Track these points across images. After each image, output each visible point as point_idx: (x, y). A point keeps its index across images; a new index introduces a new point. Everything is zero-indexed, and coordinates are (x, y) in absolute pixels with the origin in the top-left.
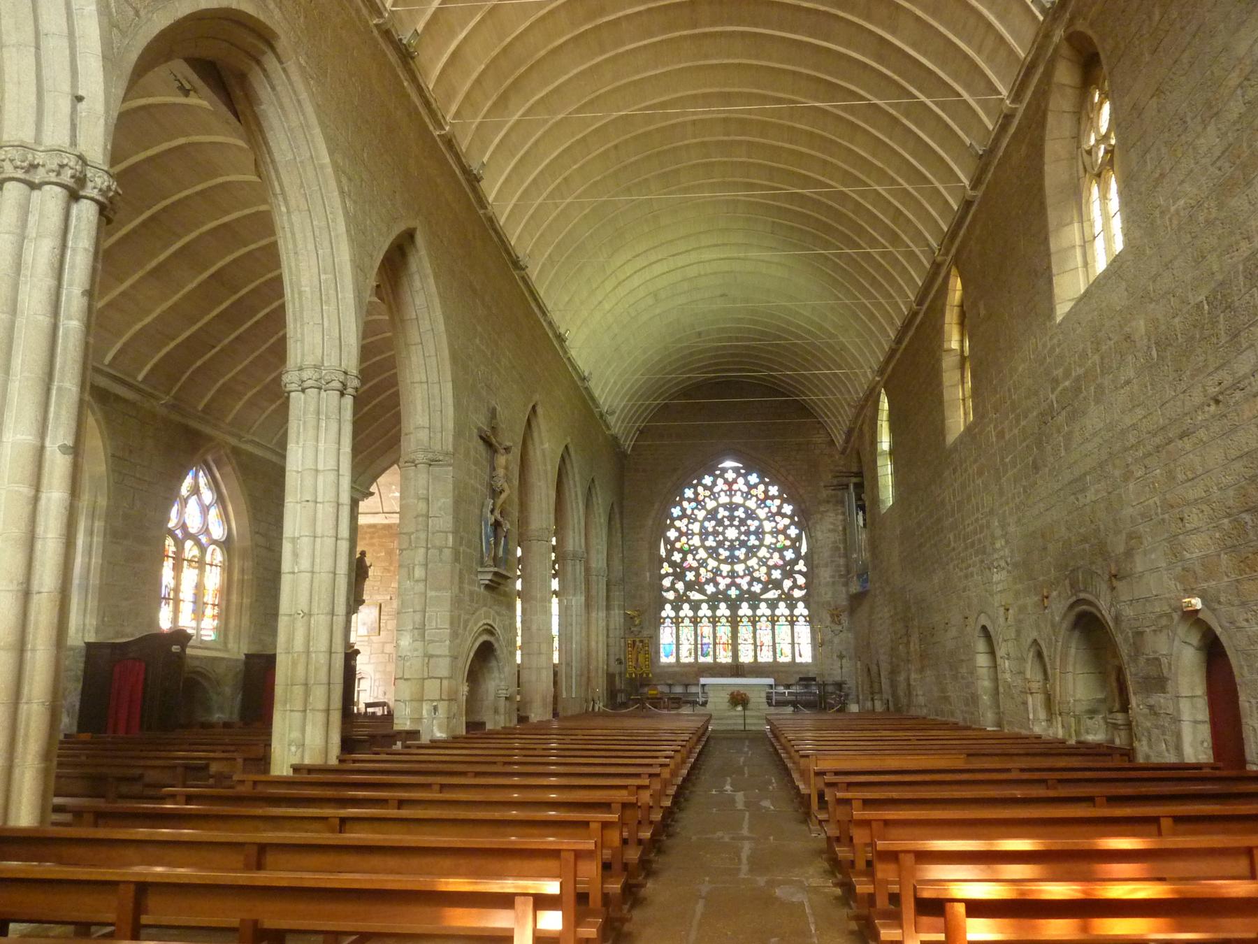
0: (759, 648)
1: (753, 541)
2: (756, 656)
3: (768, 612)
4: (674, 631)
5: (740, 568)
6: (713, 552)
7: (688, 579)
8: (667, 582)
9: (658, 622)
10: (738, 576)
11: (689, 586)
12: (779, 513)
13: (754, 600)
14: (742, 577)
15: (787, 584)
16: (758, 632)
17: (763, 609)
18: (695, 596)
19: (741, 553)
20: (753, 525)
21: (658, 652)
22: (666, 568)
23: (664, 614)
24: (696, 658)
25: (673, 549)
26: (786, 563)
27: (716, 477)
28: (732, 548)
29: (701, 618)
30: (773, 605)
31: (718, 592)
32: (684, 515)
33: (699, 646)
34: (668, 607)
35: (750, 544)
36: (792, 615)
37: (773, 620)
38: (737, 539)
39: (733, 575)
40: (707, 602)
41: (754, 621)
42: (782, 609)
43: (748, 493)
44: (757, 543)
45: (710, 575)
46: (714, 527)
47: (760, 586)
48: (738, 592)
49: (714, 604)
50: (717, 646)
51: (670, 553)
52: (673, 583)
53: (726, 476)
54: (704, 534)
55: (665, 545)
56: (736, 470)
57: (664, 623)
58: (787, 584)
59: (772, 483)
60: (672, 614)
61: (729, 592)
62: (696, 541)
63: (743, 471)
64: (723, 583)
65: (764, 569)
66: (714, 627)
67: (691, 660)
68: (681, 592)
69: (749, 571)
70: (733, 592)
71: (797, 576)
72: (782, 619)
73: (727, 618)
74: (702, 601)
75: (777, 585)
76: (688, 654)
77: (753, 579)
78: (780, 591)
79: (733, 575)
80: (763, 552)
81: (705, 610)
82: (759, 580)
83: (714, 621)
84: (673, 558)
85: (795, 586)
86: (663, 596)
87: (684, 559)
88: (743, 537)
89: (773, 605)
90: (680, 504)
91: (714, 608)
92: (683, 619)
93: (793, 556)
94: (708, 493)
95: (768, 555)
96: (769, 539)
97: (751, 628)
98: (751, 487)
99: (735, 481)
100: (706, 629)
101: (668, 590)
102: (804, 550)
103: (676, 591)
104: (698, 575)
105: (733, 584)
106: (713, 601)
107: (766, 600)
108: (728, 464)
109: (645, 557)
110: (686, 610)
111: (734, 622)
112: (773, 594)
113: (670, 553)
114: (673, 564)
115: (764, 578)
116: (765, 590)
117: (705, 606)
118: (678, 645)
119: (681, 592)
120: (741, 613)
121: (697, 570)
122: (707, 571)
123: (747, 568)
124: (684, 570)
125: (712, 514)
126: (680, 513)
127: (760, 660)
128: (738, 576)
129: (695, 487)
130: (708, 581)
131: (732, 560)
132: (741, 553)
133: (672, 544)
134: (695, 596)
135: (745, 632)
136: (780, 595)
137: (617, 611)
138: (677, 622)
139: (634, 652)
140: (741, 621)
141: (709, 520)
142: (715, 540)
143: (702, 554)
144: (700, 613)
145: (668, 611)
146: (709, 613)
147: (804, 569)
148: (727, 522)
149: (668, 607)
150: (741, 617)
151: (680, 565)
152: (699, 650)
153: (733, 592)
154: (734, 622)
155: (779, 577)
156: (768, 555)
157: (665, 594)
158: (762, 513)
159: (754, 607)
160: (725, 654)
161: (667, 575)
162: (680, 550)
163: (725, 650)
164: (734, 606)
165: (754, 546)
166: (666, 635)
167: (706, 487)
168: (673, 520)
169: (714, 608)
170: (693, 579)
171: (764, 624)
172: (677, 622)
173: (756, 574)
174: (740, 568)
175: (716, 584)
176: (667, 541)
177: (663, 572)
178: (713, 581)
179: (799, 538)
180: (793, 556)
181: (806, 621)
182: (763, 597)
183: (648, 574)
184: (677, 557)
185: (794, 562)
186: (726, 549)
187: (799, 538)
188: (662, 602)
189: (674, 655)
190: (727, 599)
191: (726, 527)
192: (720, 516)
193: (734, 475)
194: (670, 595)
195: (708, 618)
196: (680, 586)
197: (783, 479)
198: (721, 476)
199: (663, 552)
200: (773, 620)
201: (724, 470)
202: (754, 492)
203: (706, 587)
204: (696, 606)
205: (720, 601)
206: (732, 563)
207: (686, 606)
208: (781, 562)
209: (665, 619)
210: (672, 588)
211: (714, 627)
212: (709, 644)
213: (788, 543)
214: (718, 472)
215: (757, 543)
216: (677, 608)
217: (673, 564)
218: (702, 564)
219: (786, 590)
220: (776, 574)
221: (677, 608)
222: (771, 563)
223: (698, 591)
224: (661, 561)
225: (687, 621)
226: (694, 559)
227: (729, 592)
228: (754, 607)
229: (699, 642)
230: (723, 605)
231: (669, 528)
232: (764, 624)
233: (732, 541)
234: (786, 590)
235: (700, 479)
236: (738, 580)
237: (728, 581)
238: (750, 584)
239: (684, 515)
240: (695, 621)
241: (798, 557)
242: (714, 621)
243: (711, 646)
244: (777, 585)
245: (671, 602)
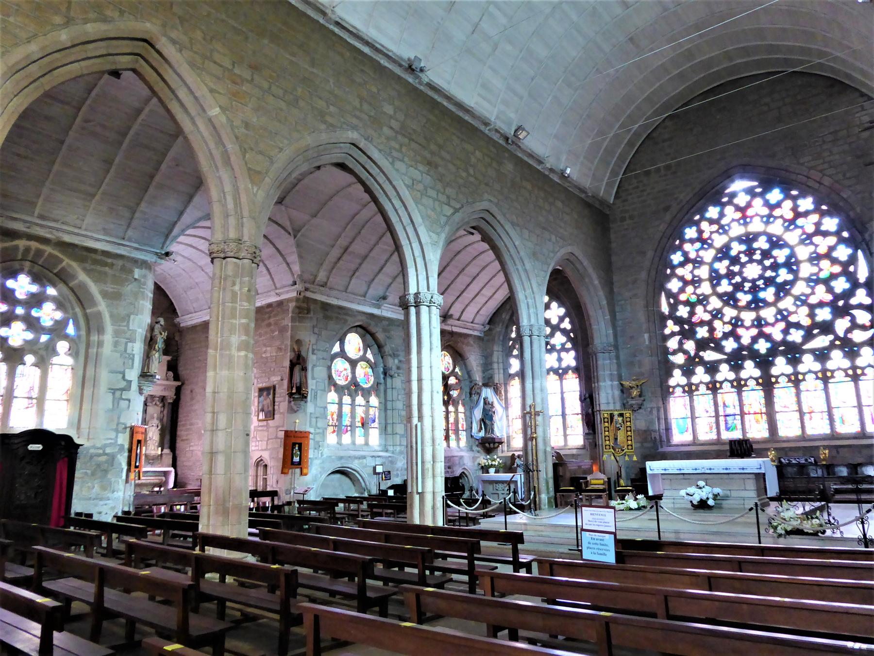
1: (784, 275)
2: (803, 427)
3: (817, 366)
4: (688, 402)
5: (768, 314)
6: (730, 299)
8: (673, 344)
9: (666, 392)
10: (767, 324)
11: (702, 345)
12: (818, 232)
13: (793, 353)
14: (773, 325)
15: (841, 325)
16: (803, 396)
17: (808, 363)
18: (710, 356)
19: (769, 294)
20: (781, 255)
21: (668, 429)
22: (671, 327)
23: (672, 382)
24: (719, 433)
25: (678, 302)
26: (837, 297)
27: (723, 205)
28: (754, 289)
29: (721, 383)
30: (822, 355)
31: (741, 348)
32: (687, 260)
33: (722, 419)
34: (677, 373)
35: (779, 280)
36: (854, 368)
37: (825, 377)
38: (761, 277)
39: (759, 323)
40: (727, 361)
41: (796, 381)
42: (837, 359)
43: (770, 216)
44: (790, 277)
45: (728, 328)
46: (728, 268)
47: (801, 333)
48: (768, 345)
49: (736, 363)
50: (747, 417)
51: (673, 308)
52: (681, 343)
53: (736, 201)
54: (715, 278)
55: (668, 298)
56: (750, 192)
57: (673, 393)
58: (841, 325)
59: (803, 195)
60: (683, 381)
61: (756, 347)
62: (705, 288)
63: (759, 190)
64: (746, 336)
65: (805, 310)
66: (739, 393)
67: (714, 436)
68: (692, 353)
69: (783, 316)
70: (762, 346)
72: (839, 375)
74: (720, 362)
75: (826, 328)
76: (708, 430)
77: (790, 325)
78: (831, 337)
79: (759, 323)
80: (800, 288)
81: (725, 372)
82: (798, 326)
83: (739, 385)
84: (678, 314)
85: (854, 326)
86: (667, 361)
87: (692, 313)
88: (769, 274)
89: (822, 355)
90: (680, 248)
91: (737, 368)
92: (697, 386)
93: (847, 286)
94: (715, 227)
95: (808, 291)
96: (806, 270)
97: (793, 390)
98: (772, 207)
99: (749, 205)
100: (728, 396)
101: (675, 353)
102: (863, 273)
103: (685, 352)
104: (712, 330)
105: (761, 335)
106: (736, 360)
107: (812, 351)
108: (739, 185)
109: (642, 316)
110: (700, 375)
111: (767, 385)
112: (822, 341)
113: (673, 308)
114: (679, 321)
115: (806, 322)
116: (809, 336)
117: (724, 368)
118: (693, 418)
119: (692, 353)
120: (774, 371)
121: (709, 324)
122: (724, 323)
123: (780, 312)
124: (693, 326)
125: (724, 253)
126: (682, 259)
127: (810, 431)
128: (767, 324)
129: (697, 224)
130: (726, 336)
131: (756, 304)
132: (769, 294)
133: (675, 296)
134: (710, 356)
135: (784, 395)
136: (832, 343)
137: (609, 383)
138: (690, 390)
139: (611, 428)
140: (777, 382)
141: (720, 260)
142: (730, 284)
143: (715, 303)
144: (719, 377)
145: (677, 378)
146: (732, 376)
147: (868, 301)
148: (744, 259)
149: (677, 373)
150: (777, 377)
151: (688, 321)
153: (762, 346)
154: (767, 385)
155: (828, 317)
156: (808, 291)
157: (671, 358)
158: (792, 237)
159: (794, 361)
161: (673, 334)
162: (687, 303)
164: (764, 363)
165: (786, 283)
166: (677, 406)
167: (711, 222)
168: (673, 268)
169: (737, 368)
171: (811, 384)
172: (690, 390)
173: (793, 319)
174: (768, 314)
175: (737, 338)
176: (670, 295)
177: (667, 331)
178: (733, 334)
179: (853, 260)
180: (847, 286)
182: (804, 347)
183: (646, 336)
184: (683, 312)
185: (848, 294)
186: (746, 293)
187: (853, 260)
188: (668, 369)
189: (690, 430)
190: (754, 355)
191: (743, 265)
192: (733, 253)
193: (748, 198)
194: (679, 359)
195: (731, 382)
196: (690, 346)
197: (816, 186)
198: (730, 203)
199: (665, 309)
200: (825, 377)
201: (733, 195)
202: (777, 212)
203: (724, 343)
204: (712, 368)
205: (744, 358)
206: (757, 308)
207: (700, 370)
208: (829, 297)
209: (674, 387)
210: (681, 349)
211: (739, 393)
213: (837, 269)
214: (725, 200)
215: (790, 277)
216: (688, 372)
217: (679, 321)
218: (717, 314)
219: (841, 334)
220: (824, 314)
221: (688, 372)
222: (813, 300)
223: (713, 349)
224: (663, 319)
225: (703, 389)
226: (705, 311)
227: (756, 347)
228: (794, 361)
229: (721, 413)
230: (749, 365)
231: (668, 278)
232: (811, 384)
233: (754, 281)
234: (841, 334)
235: (702, 211)
236: (767, 330)
237: (754, 332)
238: (786, 332)
239: (687, 260)
240: (714, 388)
241: (855, 285)
242: (739, 385)
243: (738, 417)
244: (826, 328)
245: (680, 367)
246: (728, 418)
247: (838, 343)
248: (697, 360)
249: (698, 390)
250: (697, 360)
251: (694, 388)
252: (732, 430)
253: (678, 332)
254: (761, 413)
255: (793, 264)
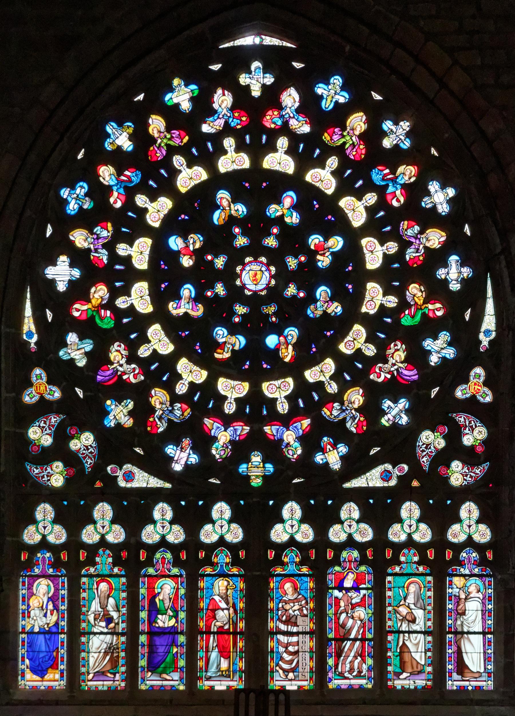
0: (332, 648)
7: (110, 422)
57: (29, 565)
68: (88, 463)
71: (461, 419)
73: (233, 548)
119: (88, 463)
122: (175, 398)
127: (334, 684)
140: (278, 561)
152: (143, 651)
160: (224, 664)
163: (224, 653)
170: (128, 422)
181: (482, 562)
212: (172, 632)
219: (425, 461)
226: (132, 358)
229: (144, 627)
234: (425, 461)
246: (158, 641)
247: (415, 483)
248: (98, 484)
249: (94, 564)
250: (98, 484)
251: (83, 555)
252: (164, 672)
253: (58, 402)
254: (235, 633)
255: (348, 277)
